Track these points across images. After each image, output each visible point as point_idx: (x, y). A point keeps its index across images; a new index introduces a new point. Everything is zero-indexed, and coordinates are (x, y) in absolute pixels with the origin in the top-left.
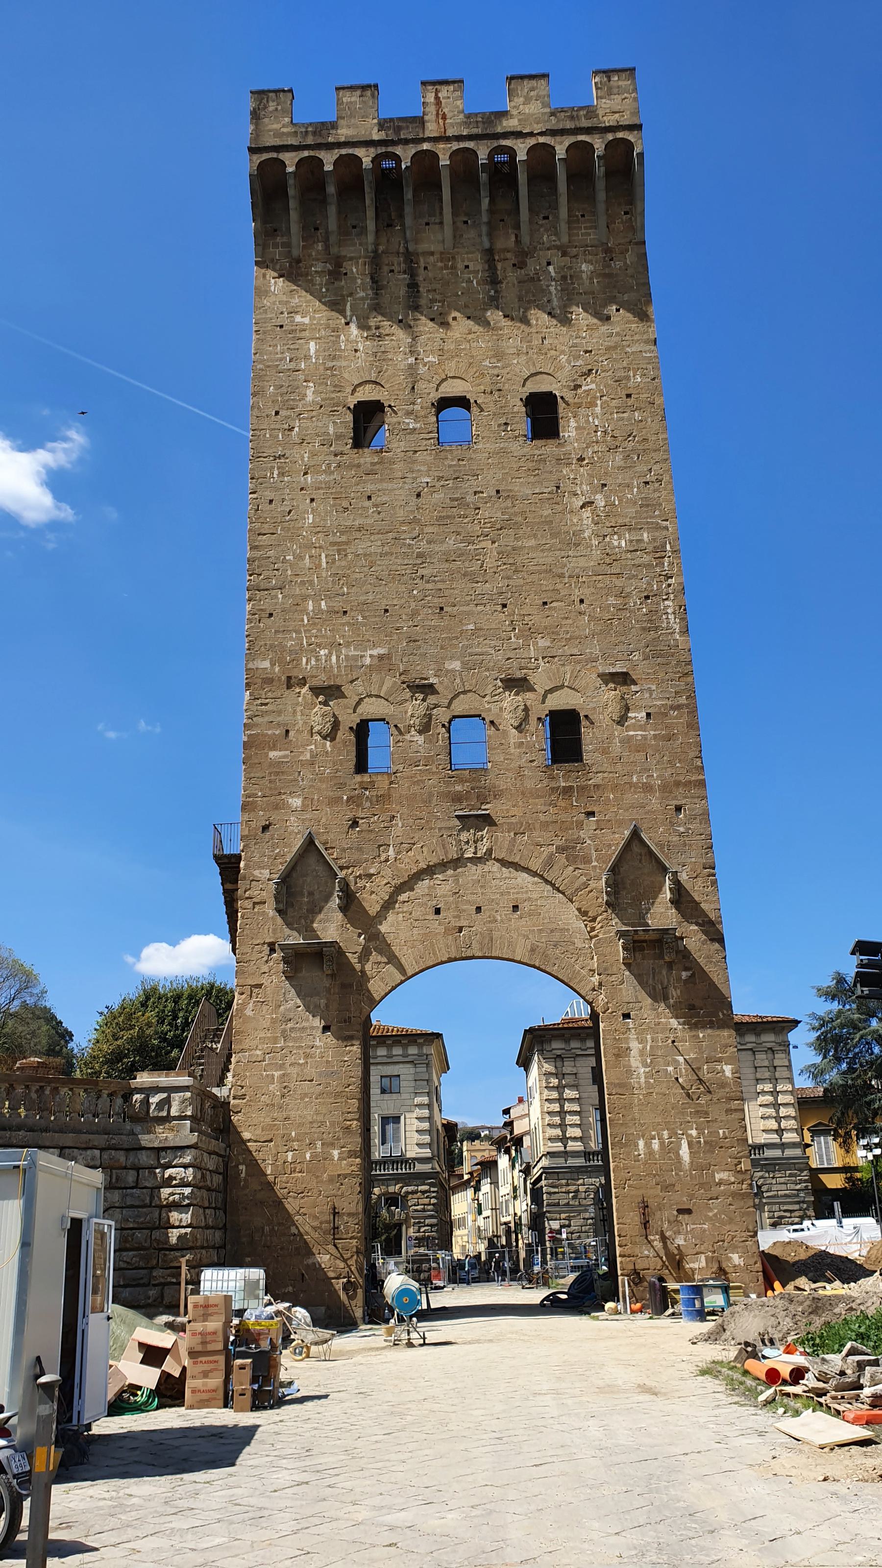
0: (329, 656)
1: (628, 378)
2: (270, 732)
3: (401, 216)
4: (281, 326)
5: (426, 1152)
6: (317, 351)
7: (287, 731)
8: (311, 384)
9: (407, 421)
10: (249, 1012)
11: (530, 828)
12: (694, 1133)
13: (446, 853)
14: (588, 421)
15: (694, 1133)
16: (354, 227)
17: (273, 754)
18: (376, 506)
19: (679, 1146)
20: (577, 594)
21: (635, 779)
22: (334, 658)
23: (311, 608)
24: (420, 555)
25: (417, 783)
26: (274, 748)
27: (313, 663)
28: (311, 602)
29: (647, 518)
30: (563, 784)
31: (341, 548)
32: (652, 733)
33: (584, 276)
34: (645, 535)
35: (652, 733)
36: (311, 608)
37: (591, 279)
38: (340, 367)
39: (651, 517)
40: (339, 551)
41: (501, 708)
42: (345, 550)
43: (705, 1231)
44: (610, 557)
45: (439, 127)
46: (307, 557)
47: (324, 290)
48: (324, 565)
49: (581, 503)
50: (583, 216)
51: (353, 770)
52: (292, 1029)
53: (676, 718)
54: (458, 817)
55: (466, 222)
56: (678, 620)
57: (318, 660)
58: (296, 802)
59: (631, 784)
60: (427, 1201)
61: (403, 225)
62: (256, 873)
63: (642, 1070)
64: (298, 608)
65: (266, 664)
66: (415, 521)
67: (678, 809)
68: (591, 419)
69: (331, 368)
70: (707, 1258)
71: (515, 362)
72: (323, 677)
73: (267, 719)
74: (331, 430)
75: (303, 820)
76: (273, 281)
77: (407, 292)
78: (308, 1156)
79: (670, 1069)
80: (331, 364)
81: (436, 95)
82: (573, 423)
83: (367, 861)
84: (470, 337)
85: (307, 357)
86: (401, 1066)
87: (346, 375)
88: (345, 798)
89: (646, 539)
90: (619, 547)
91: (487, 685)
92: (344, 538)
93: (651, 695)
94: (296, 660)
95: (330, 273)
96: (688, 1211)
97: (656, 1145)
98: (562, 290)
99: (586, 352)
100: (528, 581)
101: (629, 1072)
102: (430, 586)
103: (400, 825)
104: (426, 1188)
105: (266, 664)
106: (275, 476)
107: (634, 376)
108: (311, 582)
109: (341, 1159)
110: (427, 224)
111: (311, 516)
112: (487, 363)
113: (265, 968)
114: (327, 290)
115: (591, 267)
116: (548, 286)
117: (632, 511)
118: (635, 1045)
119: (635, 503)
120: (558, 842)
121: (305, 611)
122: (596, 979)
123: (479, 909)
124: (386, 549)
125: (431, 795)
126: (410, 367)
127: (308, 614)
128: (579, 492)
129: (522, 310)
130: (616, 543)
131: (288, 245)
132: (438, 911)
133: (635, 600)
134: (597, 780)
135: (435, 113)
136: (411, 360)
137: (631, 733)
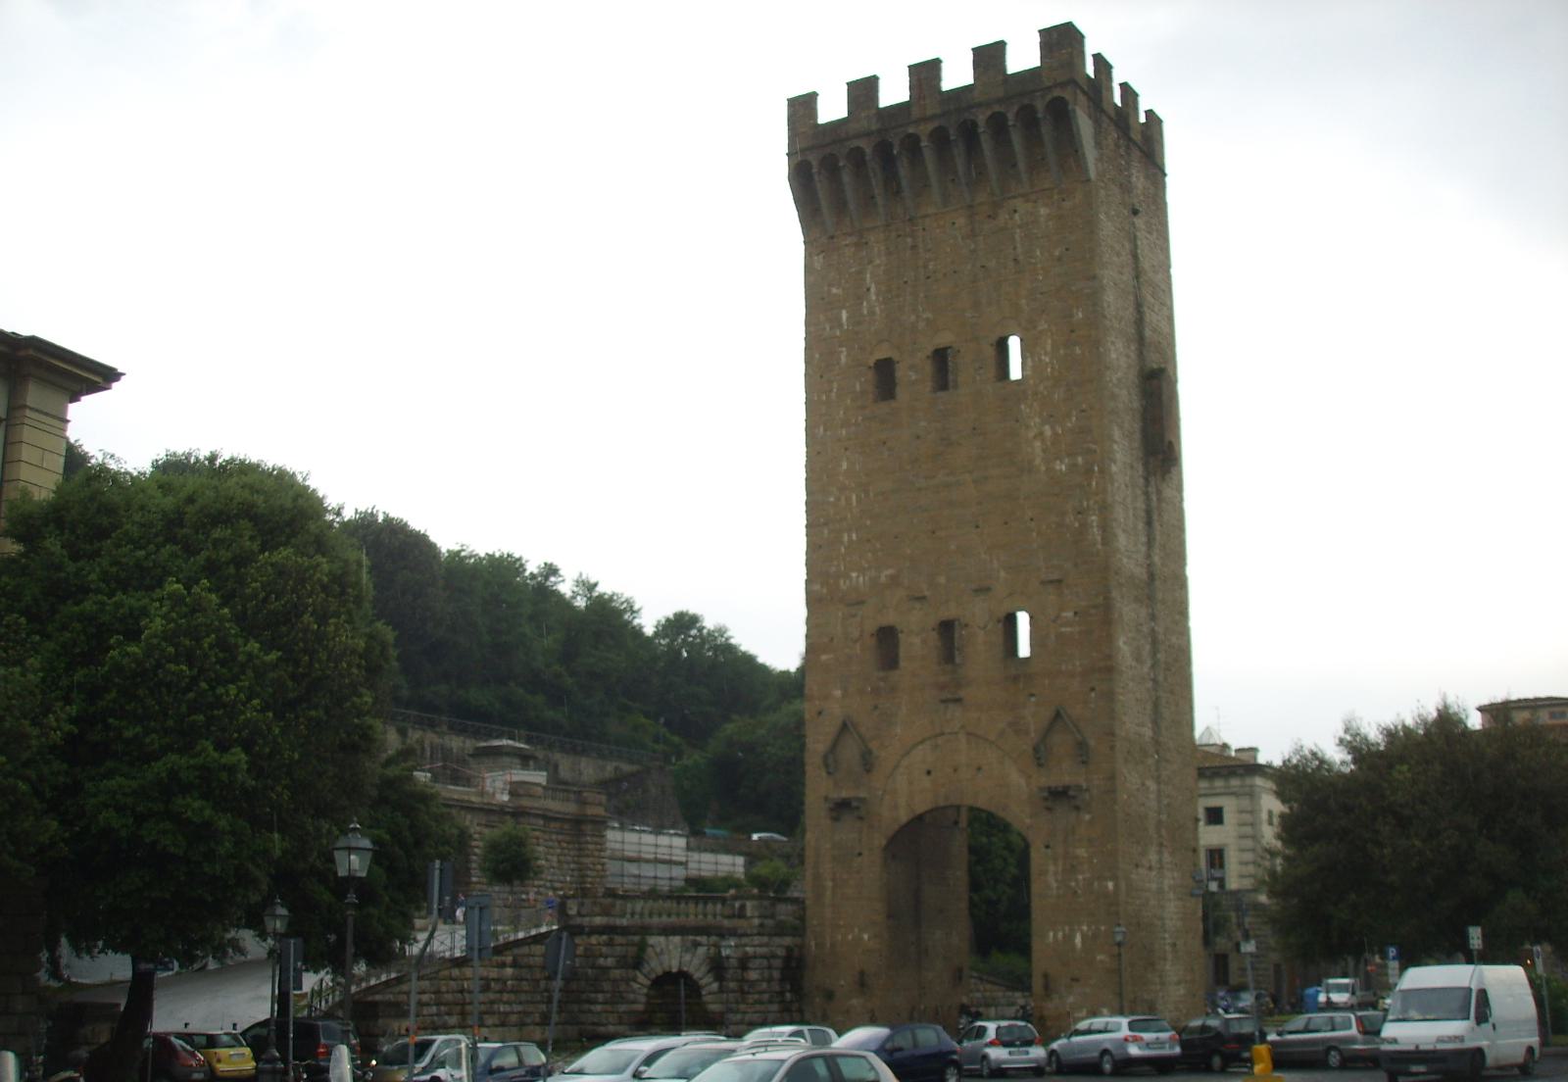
0: (858, 577)
1: (1072, 316)
6: (848, 318)
12: (1085, 928)
14: (1040, 360)
17: (824, 657)
19: (1074, 937)
22: (861, 579)
24: (919, 489)
58: (838, 693)
67: (1093, 689)
74: (858, 387)
85: (840, 325)
90: (1061, 470)
95: (856, 245)
97: (1060, 935)
105: (817, 587)
115: (1048, 211)
118: (1052, 868)
130: (1058, 468)
132: (929, 773)
133: (1070, 519)
136: (913, 318)
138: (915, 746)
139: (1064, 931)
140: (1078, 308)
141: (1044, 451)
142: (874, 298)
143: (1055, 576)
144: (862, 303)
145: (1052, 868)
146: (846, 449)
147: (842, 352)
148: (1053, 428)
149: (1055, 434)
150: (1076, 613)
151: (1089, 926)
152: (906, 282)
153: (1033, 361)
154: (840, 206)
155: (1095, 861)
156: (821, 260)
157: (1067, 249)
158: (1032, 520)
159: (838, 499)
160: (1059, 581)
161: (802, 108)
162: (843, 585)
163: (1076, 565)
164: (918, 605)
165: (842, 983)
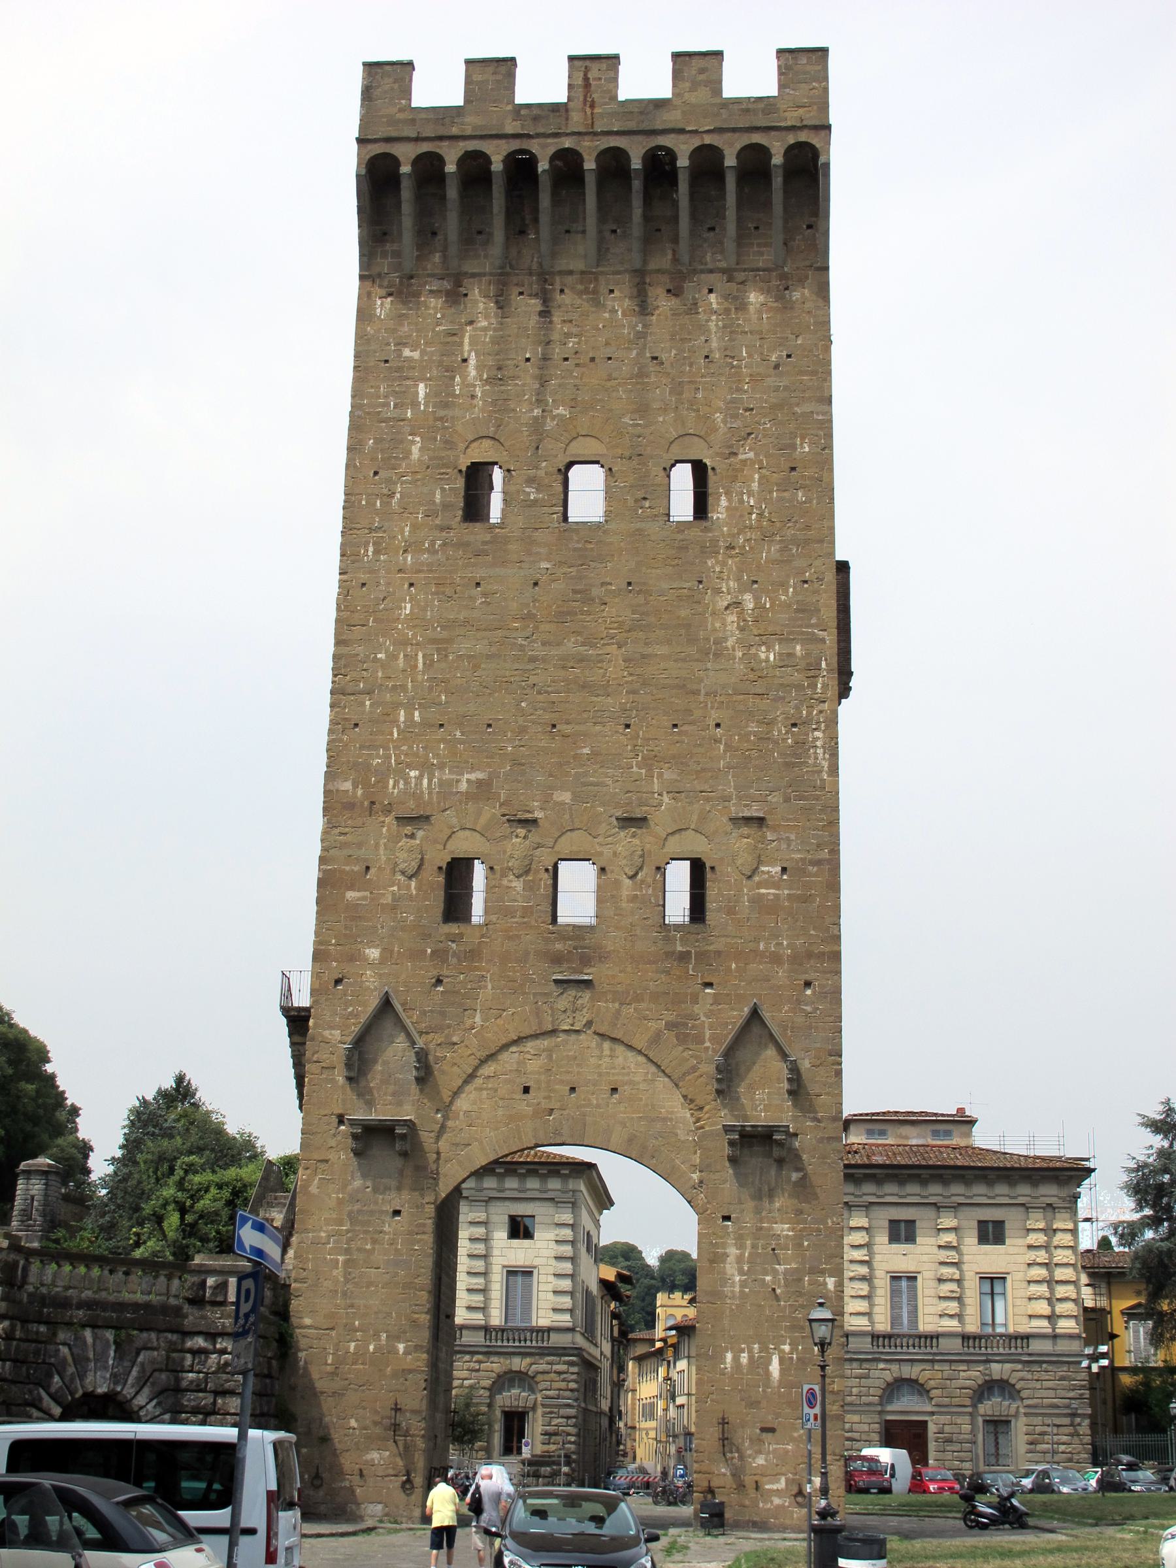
0: (421, 776)
1: (793, 447)
2: (347, 868)
3: (536, 220)
4: (386, 361)
5: (565, 1319)
7: (368, 868)
8: (418, 439)
9: (527, 490)
10: (313, 1189)
11: (638, 999)
12: (787, 1348)
13: (540, 1023)
14: (741, 501)
15: (787, 1348)
16: (480, 233)
17: (351, 895)
18: (485, 595)
19: (769, 1362)
20: (714, 716)
21: (762, 947)
22: (425, 781)
23: (402, 719)
24: (533, 659)
25: (510, 938)
26: (351, 888)
27: (401, 786)
28: (402, 712)
29: (801, 626)
30: (679, 948)
31: (442, 646)
32: (786, 892)
33: (752, 308)
34: (798, 648)
35: (786, 892)
36: (402, 719)
37: (759, 312)
38: (453, 417)
39: (808, 626)
40: (438, 650)
41: (615, 854)
42: (446, 649)
43: (787, 1452)
44: (755, 670)
45: (586, 119)
46: (402, 655)
47: (439, 316)
48: (420, 665)
49: (726, 603)
50: (757, 228)
51: (440, 919)
52: (359, 1211)
53: (816, 875)
54: (556, 981)
55: (614, 231)
56: (827, 756)
57: (407, 783)
58: (374, 953)
59: (755, 951)
60: (563, 1385)
61: (537, 233)
62: (327, 1033)
63: (737, 1279)
64: (388, 719)
65: (348, 786)
66: (530, 616)
67: (808, 984)
68: (745, 497)
69: (441, 419)
70: (787, 1481)
71: (661, 419)
72: (412, 804)
73: (346, 852)
75: (381, 975)
76: (379, 302)
77: (538, 322)
78: (371, 1348)
79: (768, 1278)
80: (441, 413)
81: (586, 75)
82: (724, 502)
83: (449, 1026)
84: (609, 384)
85: (415, 404)
86: (538, 1204)
87: (459, 428)
88: (429, 951)
89: (799, 653)
90: (767, 660)
91: (600, 823)
92: (445, 634)
93: (789, 845)
94: (383, 782)
96: (772, 1430)
97: (744, 1358)
98: (724, 327)
99: (747, 410)
100: (658, 697)
101: (725, 1280)
102: (541, 698)
103: (490, 987)
104: (564, 1367)
105: (348, 786)
106: (370, 553)
107: (801, 444)
108: (403, 687)
109: (406, 1353)
110: (568, 232)
111: (408, 606)
112: (626, 420)
113: (333, 1143)
114: (443, 316)
116: (707, 321)
117: (783, 617)
118: (733, 1251)
119: (790, 606)
120: (670, 1016)
121: (395, 722)
122: (695, 1176)
123: (573, 1089)
124: (494, 649)
125: (527, 953)
126: (536, 418)
127: (398, 727)
128: (724, 590)
129: (674, 352)
130: (763, 656)
131: (397, 254)
132: (526, 1090)
134: (718, 945)
135: (581, 99)
137: (763, 891)
138: (505, 1047)
139: (750, 1351)
140: (803, 438)
141: (742, 629)
142: (473, 373)
143: (755, 811)
144: (453, 378)
145: (733, 1251)
146: (411, 585)
147: (413, 442)
148: (757, 599)
149: (759, 606)
150: (784, 870)
151: (794, 1345)
152: (528, 360)
153: (729, 500)
154: (427, 234)
155: (806, 1243)
156: (388, 306)
157: (789, 356)
158: (718, 725)
159: (393, 657)
160: (761, 821)
161: (386, 80)
162: (394, 787)
163: (787, 800)
164: (521, 832)
165: (353, 1423)
